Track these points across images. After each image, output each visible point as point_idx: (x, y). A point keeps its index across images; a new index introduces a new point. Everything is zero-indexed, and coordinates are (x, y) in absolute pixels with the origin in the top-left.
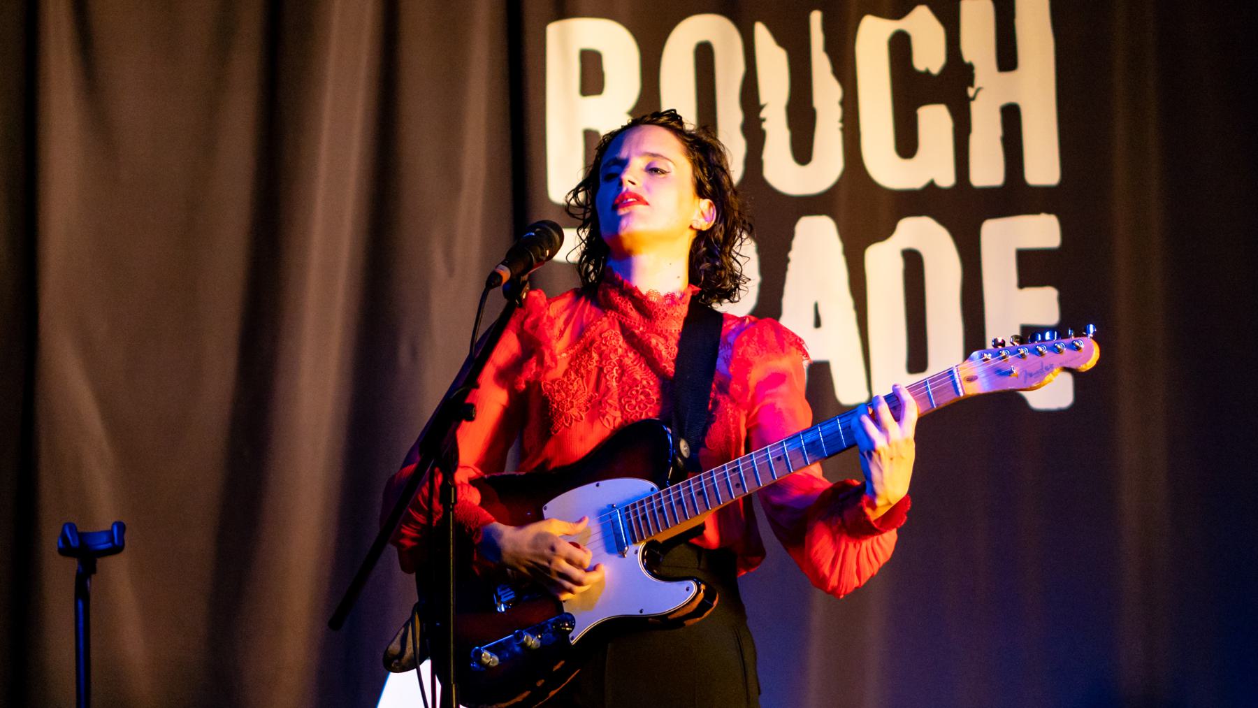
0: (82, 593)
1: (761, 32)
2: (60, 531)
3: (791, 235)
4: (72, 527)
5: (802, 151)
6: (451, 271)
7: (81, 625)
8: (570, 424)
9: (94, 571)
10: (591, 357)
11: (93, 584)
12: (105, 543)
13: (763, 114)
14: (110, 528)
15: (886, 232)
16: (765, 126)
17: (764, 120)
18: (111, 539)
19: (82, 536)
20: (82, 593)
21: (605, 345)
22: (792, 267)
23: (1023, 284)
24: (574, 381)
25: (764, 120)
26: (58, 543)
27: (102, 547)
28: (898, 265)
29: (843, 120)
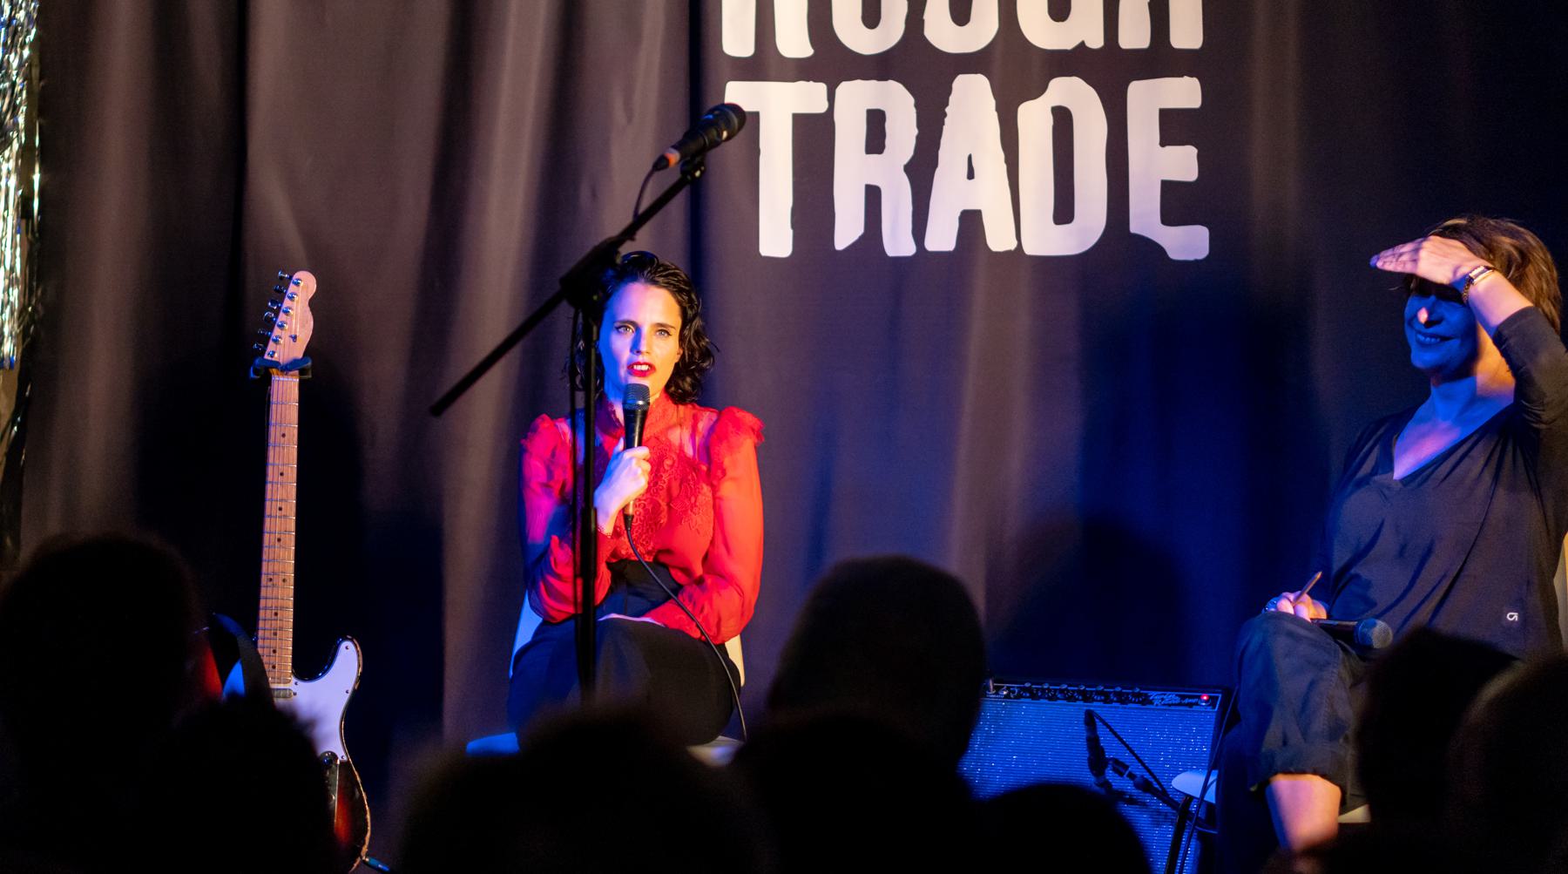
6: (630, 119)
15: (1039, 90)
22: (946, 120)
23: (1163, 144)
28: (1049, 121)
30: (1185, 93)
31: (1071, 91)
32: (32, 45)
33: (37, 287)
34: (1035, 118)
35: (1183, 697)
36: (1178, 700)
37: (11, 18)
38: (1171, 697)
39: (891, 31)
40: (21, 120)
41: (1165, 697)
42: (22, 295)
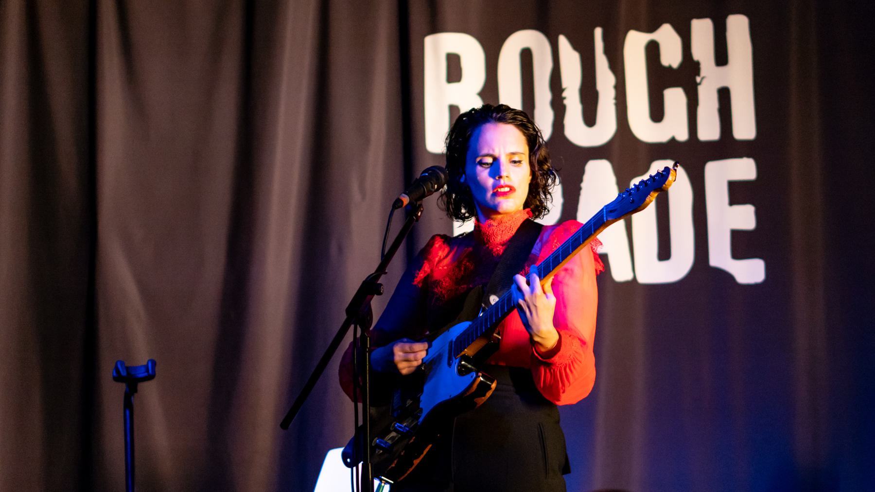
0: (128, 405)
1: (563, 41)
2: (114, 367)
3: (582, 172)
4: (122, 363)
5: (590, 118)
6: (364, 197)
7: (128, 425)
9: (136, 391)
11: (135, 400)
12: (143, 373)
13: (564, 94)
14: (145, 363)
16: (566, 102)
17: (565, 98)
18: (147, 371)
19: (127, 368)
20: (128, 405)
25: (565, 98)
26: (113, 373)
27: (141, 375)
29: (616, 98)
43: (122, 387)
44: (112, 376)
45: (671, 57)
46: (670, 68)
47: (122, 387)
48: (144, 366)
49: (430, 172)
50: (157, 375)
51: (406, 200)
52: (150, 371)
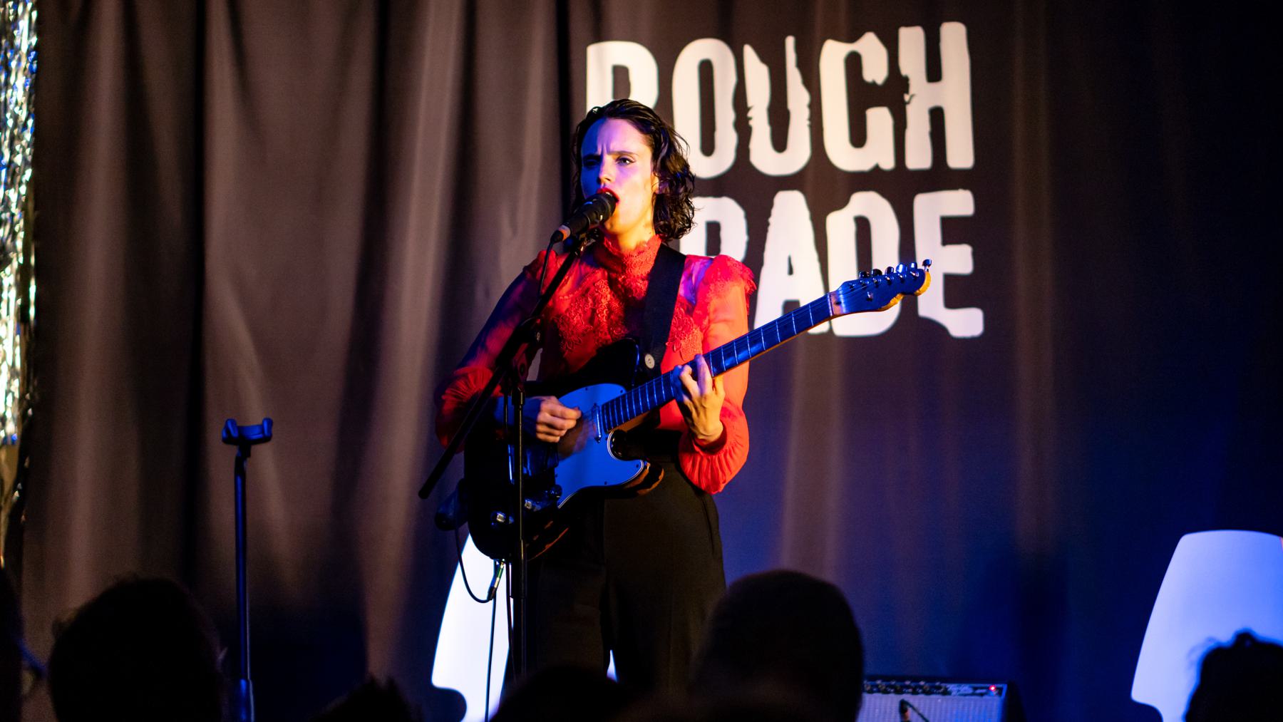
0: (240, 471)
3: (770, 205)
4: (233, 422)
6: (515, 231)
7: (240, 496)
8: (572, 348)
9: (249, 455)
10: (587, 301)
11: (248, 465)
13: (750, 114)
14: (260, 422)
15: (842, 203)
16: (751, 123)
17: (750, 119)
18: (263, 431)
19: (241, 429)
20: (240, 471)
21: (597, 292)
24: (574, 317)
25: (750, 119)
27: (255, 437)
28: (851, 229)
30: (960, 203)
31: (869, 204)
32: (28, 184)
33: (35, 377)
34: (840, 225)
35: (975, 689)
36: (971, 691)
37: (11, 162)
38: (966, 688)
39: (723, 159)
40: (19, 244)
41: (960, 688)
42: (22, 385)
43: (233, 451)
44: (221, 438)
45: (875, 71)
46: (874, 84)
47: (233, 451)
48: (258, 426)
49: (595, 200)
50: (274, 436)
51: (566, 232)
52: (266, 432)
